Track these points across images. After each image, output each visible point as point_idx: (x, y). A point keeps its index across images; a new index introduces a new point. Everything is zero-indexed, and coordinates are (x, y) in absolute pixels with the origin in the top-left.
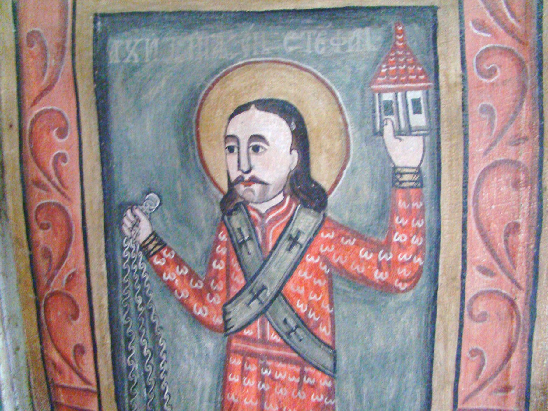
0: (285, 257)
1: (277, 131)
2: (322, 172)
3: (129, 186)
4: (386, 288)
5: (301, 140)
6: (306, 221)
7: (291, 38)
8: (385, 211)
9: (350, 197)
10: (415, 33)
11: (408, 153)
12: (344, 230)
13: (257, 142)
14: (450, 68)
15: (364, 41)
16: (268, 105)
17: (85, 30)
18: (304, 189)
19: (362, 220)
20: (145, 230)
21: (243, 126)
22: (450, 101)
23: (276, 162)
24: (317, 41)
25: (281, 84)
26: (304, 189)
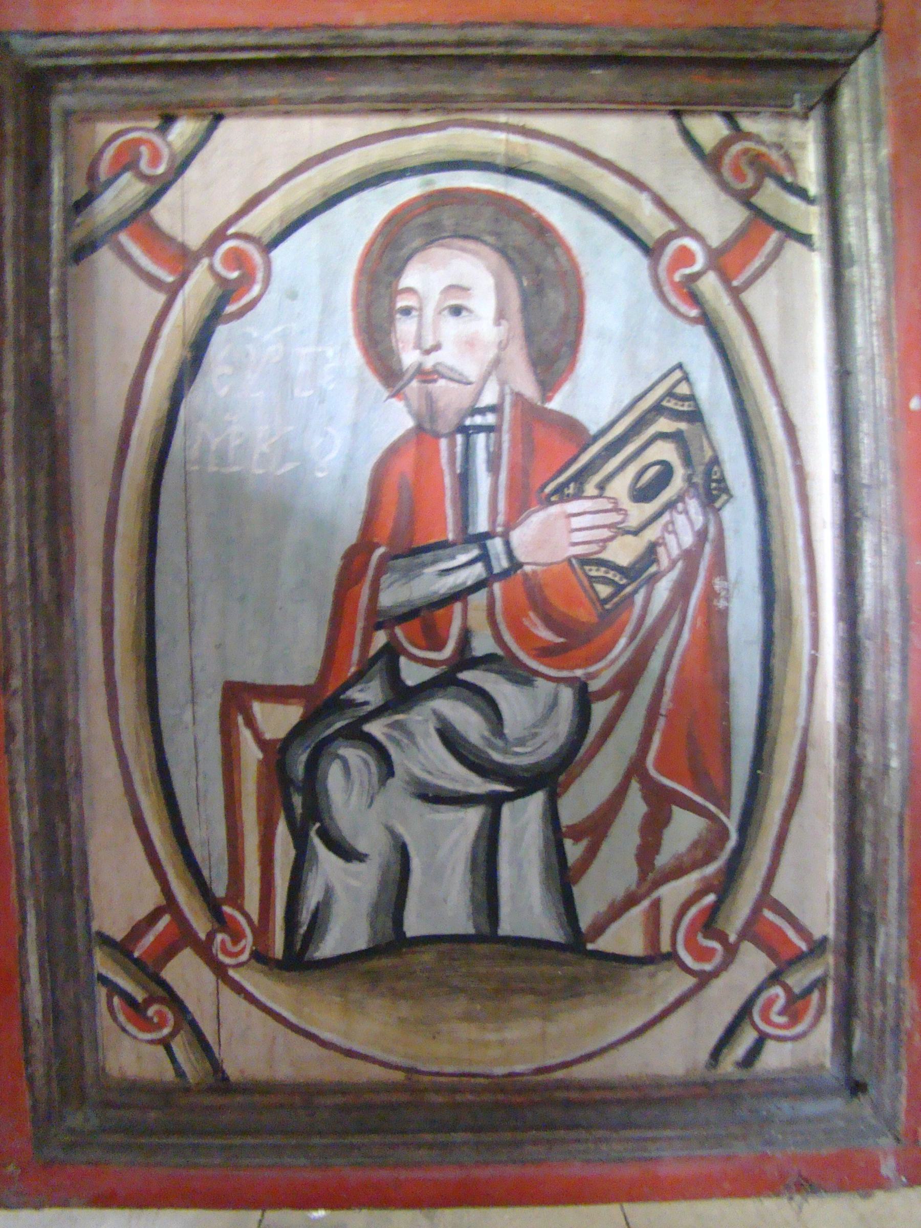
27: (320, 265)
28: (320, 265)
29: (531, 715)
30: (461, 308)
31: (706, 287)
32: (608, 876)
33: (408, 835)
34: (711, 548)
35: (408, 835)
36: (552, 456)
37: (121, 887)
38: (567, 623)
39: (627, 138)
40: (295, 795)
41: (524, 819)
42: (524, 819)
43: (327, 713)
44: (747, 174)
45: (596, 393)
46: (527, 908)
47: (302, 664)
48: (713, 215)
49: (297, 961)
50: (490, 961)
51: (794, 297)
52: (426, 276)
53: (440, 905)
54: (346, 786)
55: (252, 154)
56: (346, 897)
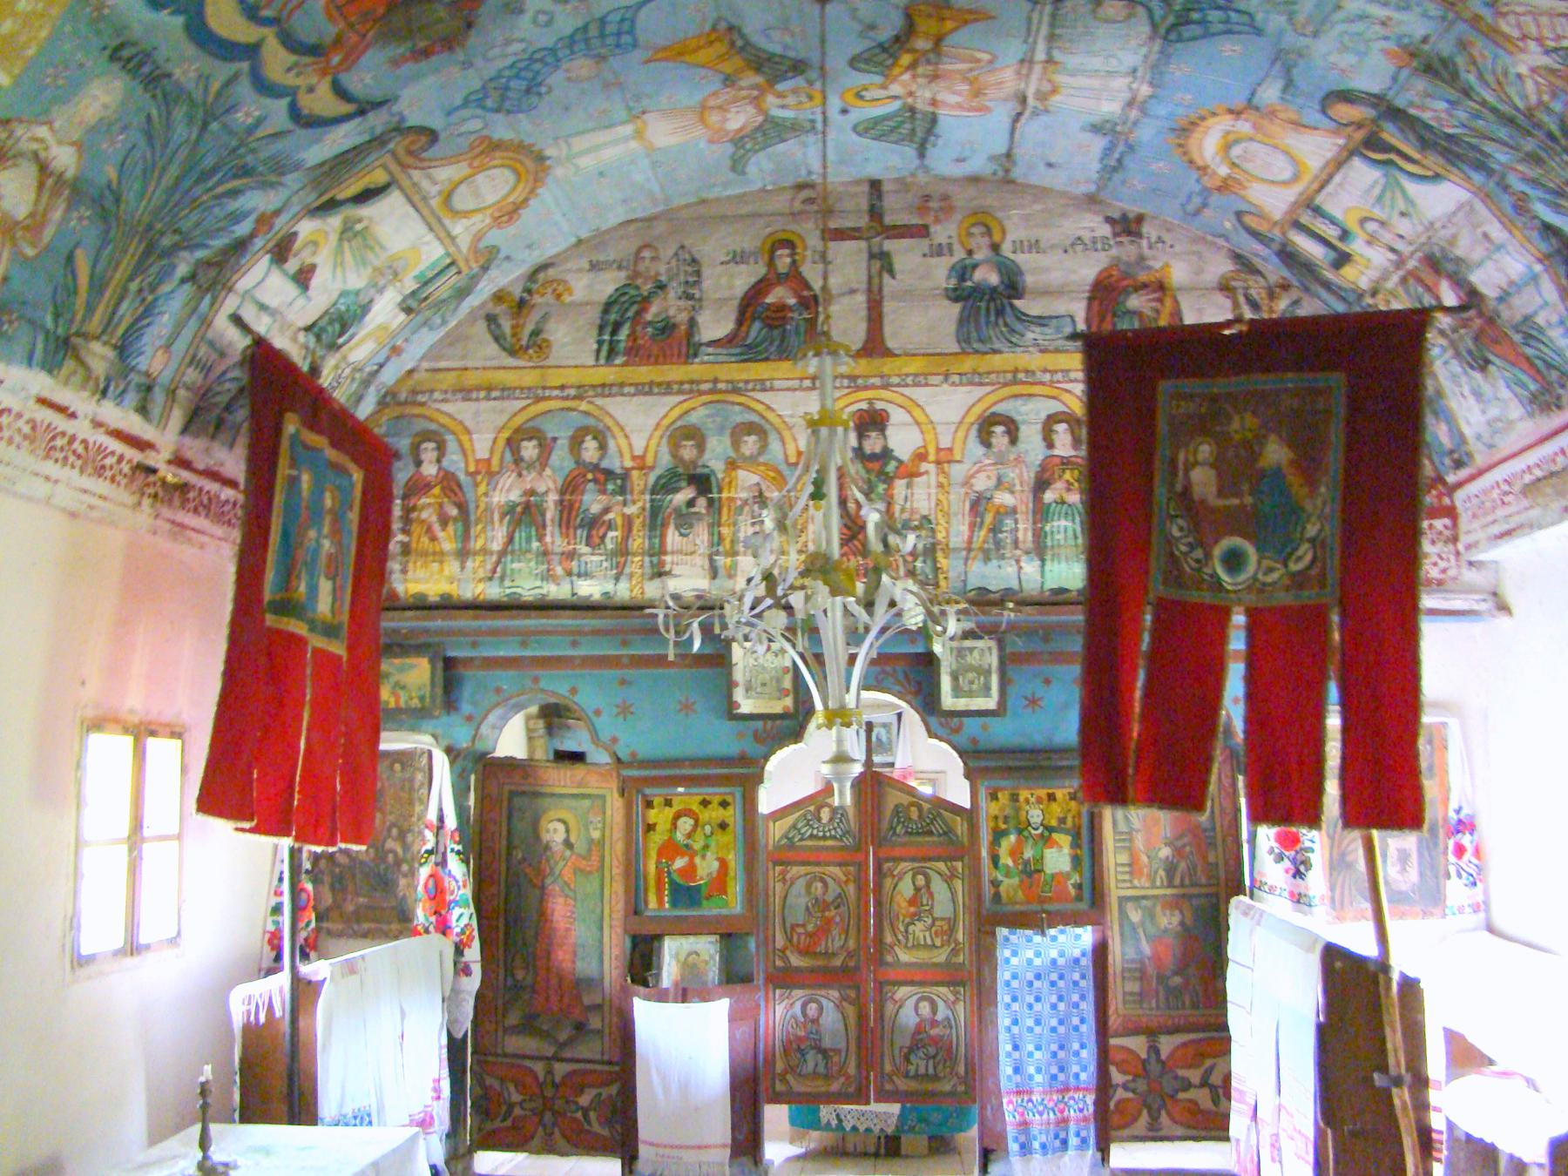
0: (562, 864)
1: (561, 827)
2: (573, 839)
3: (516, 842)
4: (590, 873)
5: (567, 831)
6: (568, 853)
7: (566, 801)
8: (590, 850)
9: (580, 847)
10: (599, 802)
11: (596, 835)
12: (579, 855)
13: (555, 830)
14: (609, 812)
15: (587, 803)
16: (559, 820)
17: (506, 795)
18: (568, 844)
19: (584, 852)
20: (520, 856)
21: (551, 826)
22: (608, 820)
23: (559, 837)
24: (573, 803)
25: (563, 814)
26: (568, 844)
27: (910, 1003)
28: (910, 1003)
29: (932, 1051)
30: (925, 1008)
31: (951, 1006)
32: (940, 1067)
33: (919, 1064)
34: (950, 1035)
35: (919, 1064)
36: (934, 1023)
37: (888, 1068)
38: (935, 1041)
39: (943, 990)
40: (908, 1060)
41: (931, 1062)
42: (931, 1062)
43: (911, 1050)
44: (956, 993)
45: (939, 1017)
46: (931, 1071)
47: (908, 1043)
48: (952, 998)
49: (906, 1076)
50: (926, 1077)
51: (960, 1007)
52: (922, 1005)
53: (922, 1071)
54: (912, 1058)
55: (902, 991)
56: (912, 1069)
